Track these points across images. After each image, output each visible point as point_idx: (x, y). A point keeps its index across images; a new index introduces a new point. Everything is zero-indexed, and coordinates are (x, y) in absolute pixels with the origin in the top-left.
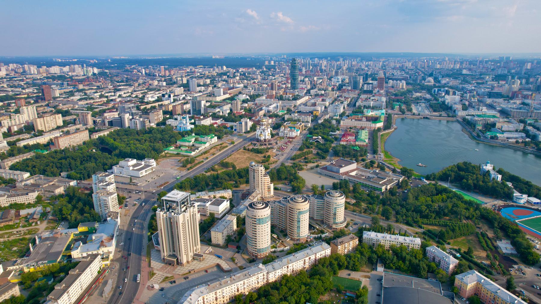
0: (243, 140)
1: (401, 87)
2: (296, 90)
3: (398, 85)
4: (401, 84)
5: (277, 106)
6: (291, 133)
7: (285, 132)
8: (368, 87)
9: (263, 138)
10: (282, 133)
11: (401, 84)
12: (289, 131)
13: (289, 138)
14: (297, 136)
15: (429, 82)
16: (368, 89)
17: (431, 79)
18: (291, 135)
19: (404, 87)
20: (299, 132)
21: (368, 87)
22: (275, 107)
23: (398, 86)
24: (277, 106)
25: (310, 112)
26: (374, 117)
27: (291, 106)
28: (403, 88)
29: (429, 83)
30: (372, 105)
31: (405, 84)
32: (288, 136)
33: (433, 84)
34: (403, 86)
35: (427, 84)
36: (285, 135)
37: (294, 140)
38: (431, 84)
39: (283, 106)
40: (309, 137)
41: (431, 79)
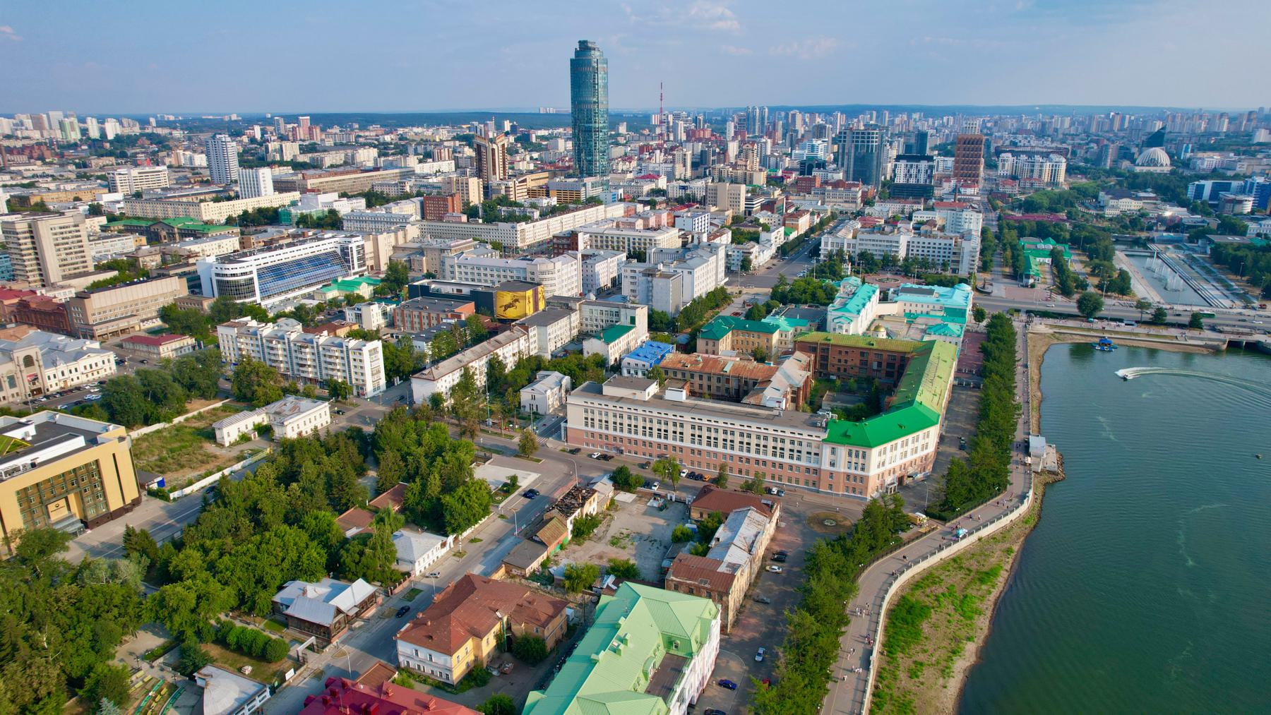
1: (1046, 178)
2: (589, 181)
3: (1037, 168)
4: (1047, 167)
5: (345, 252)
8: (913, 171)
11: (1047, 167)
15: (1153, 162)
16: (912, 181)
17: (1161, 154)
19: (1062, 177)
21: (913, 171)
23: (1036, 175)
26: (879, 353)
28: (1054, 183)
29: (1152, 169)
30: (902, 254)
31: (1063, 167)
33: (1169, 168)
34: (1054, 173)
35: (1145, 169)
38: (1158, 169)
41: (1161, 154)
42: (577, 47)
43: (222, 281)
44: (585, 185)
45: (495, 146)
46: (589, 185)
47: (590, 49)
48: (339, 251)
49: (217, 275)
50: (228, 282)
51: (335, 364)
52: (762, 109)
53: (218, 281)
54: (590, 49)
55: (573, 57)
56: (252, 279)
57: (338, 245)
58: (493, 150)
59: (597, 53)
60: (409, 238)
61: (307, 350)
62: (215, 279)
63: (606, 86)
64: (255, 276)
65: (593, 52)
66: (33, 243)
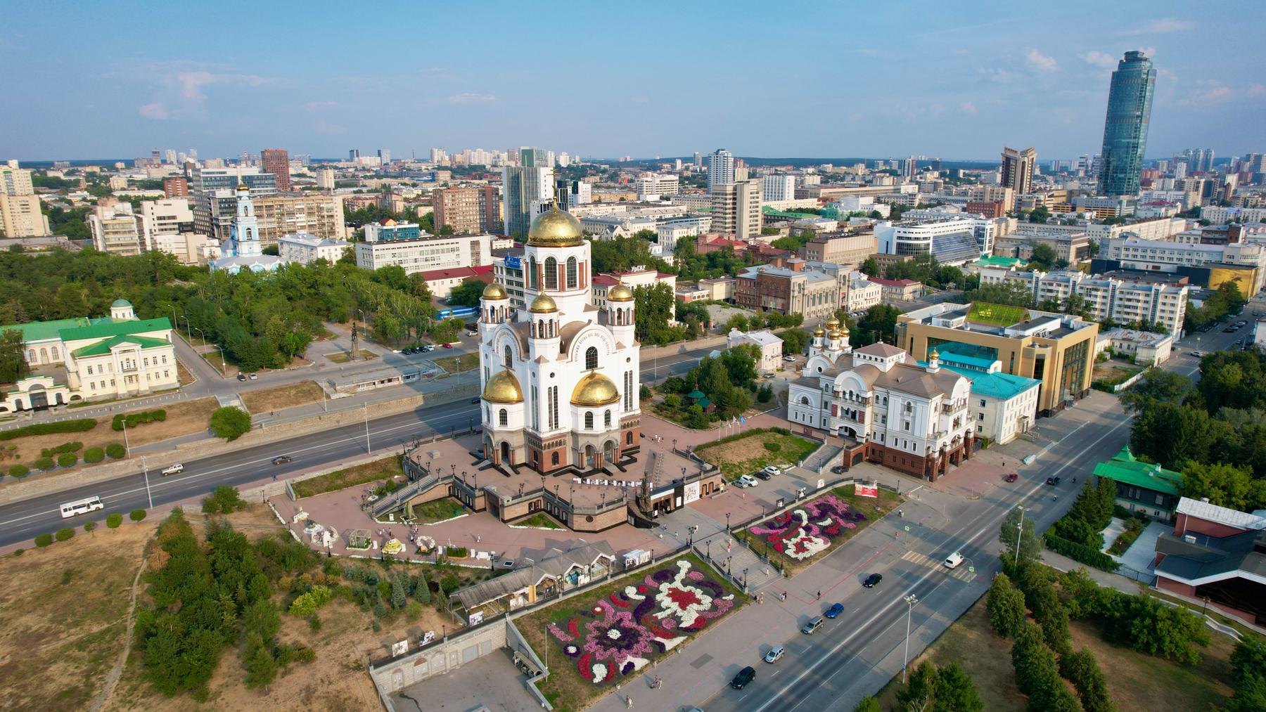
0: (420, 412)
2: (1124, 198)
5: (980, 233)
6: (896, 402)
7: (842, 382)
9: (518, 418)
10: (813, 395)
12: (882, 381)
13: (878, 455)
14: (978, 443)
18: (894, 424)
20: (1024, 404)
22: (963, 239)
24: (980, 233)
25: (1182, 271)
27: (1068, 242)
32: (866, 429)
36: (837, 424)
37: (914, 490)
39: (1022, 242)
40: (1124, 489)
42: (1123, 58)
43: (903, 244)
44: (1120, 203)
45: (1026, 160)
46: (1124, 203)
47: (1141, 60)
48: (972, 232)
49: (899, 238)
50: (910, 245)
51: (1136, 308)
52: (1207, 153)
53: (899, 244)
54: (1141, 60)
55: (1116, 69)
56: (928, 245)
57: (973, 227)
58: (1024, 163)
59: (1148, 64)
60: (1010, 230)
61: (1099, 293)
62: (895, 241)
63: (1151, 100)
64: (931, 242)
65: (1143, 63)
66: (734, 204)
